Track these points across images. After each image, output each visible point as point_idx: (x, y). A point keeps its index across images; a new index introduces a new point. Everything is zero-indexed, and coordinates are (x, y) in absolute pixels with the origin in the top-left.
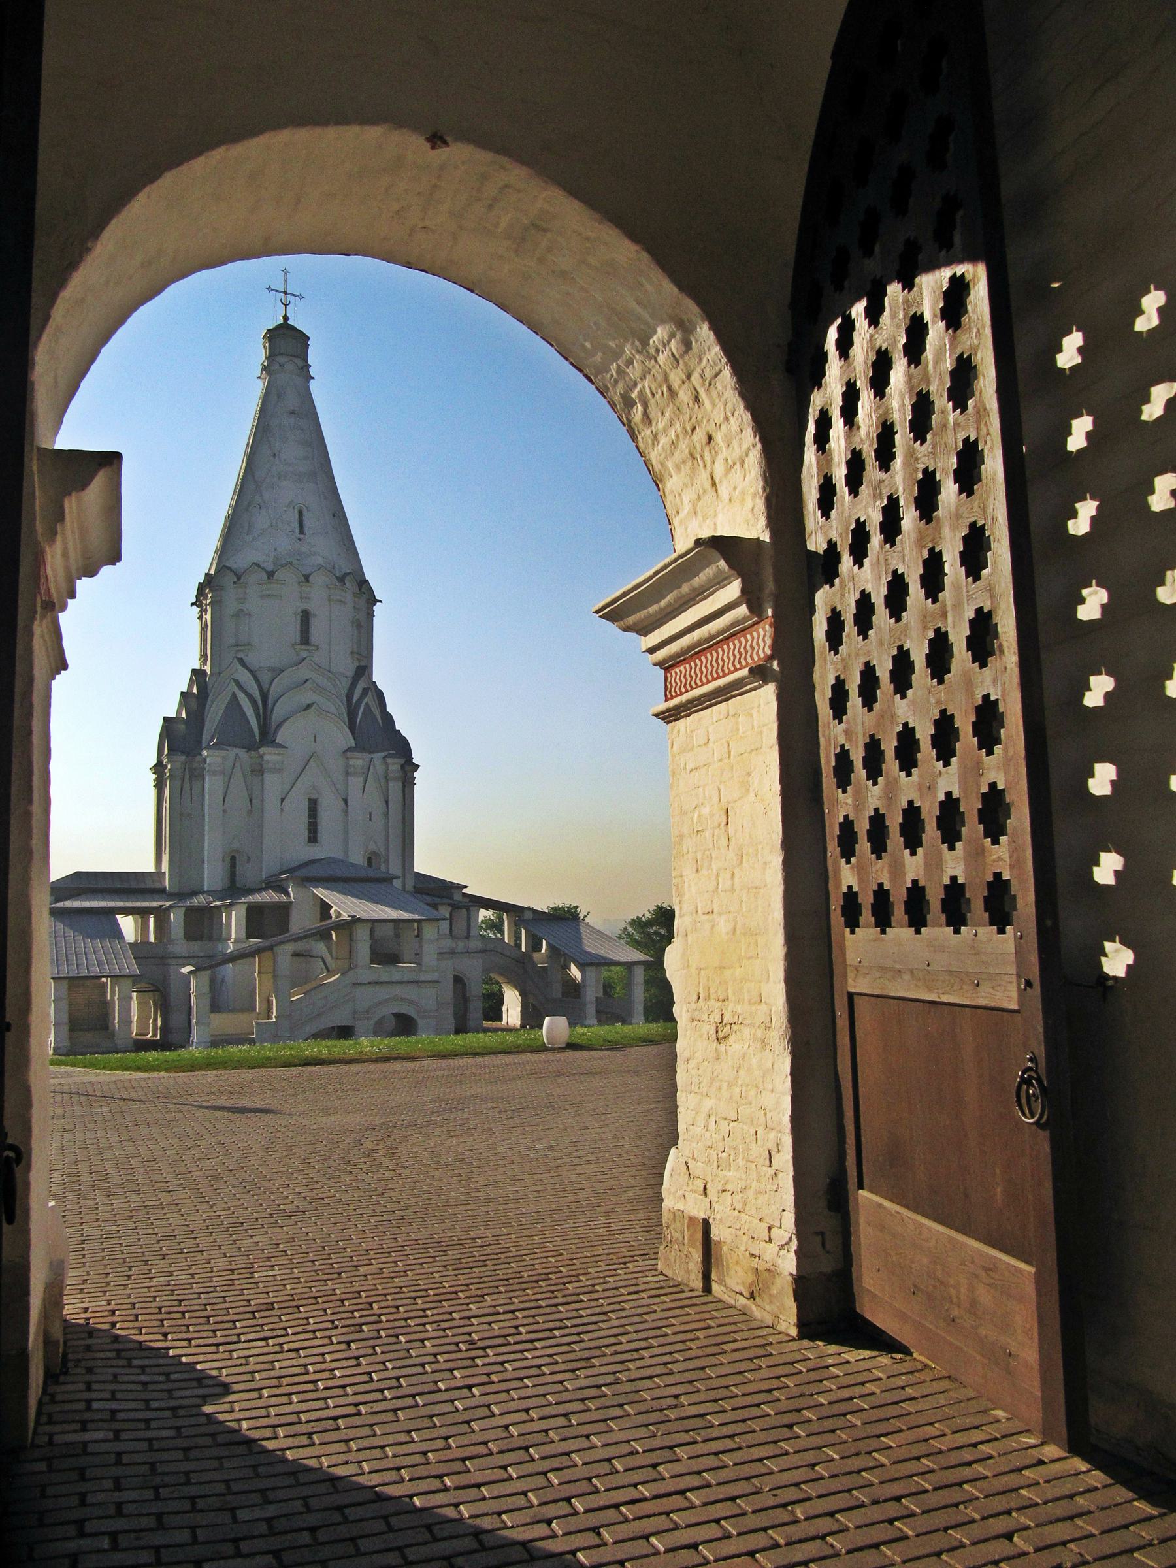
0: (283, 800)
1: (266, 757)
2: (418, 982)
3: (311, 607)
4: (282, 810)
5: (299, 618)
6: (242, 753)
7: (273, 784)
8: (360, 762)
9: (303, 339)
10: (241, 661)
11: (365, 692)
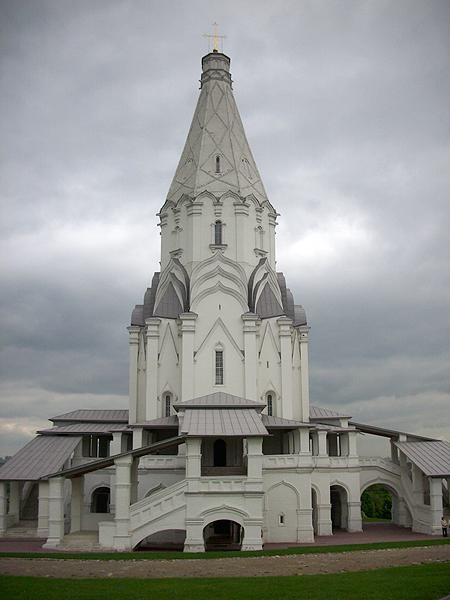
0: (195, 353)
1: (184, 323)
2: (243, 493)
3: (222, 219)
4: (195, 361)
5: (214, 228)
6: (172, 322)
7: (188, 342)
8: (253, 324)
9: (228, 60)
10: (177, 261)
11: (266, 275)
